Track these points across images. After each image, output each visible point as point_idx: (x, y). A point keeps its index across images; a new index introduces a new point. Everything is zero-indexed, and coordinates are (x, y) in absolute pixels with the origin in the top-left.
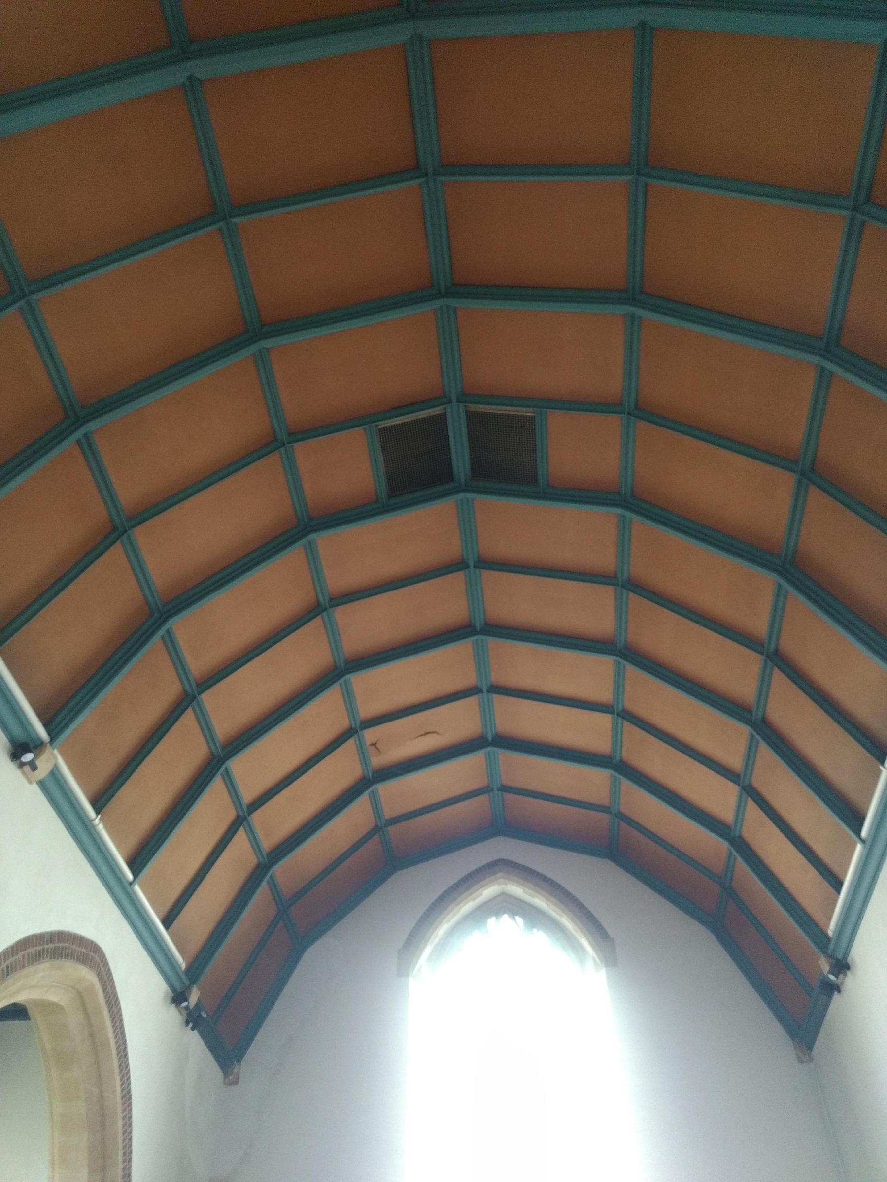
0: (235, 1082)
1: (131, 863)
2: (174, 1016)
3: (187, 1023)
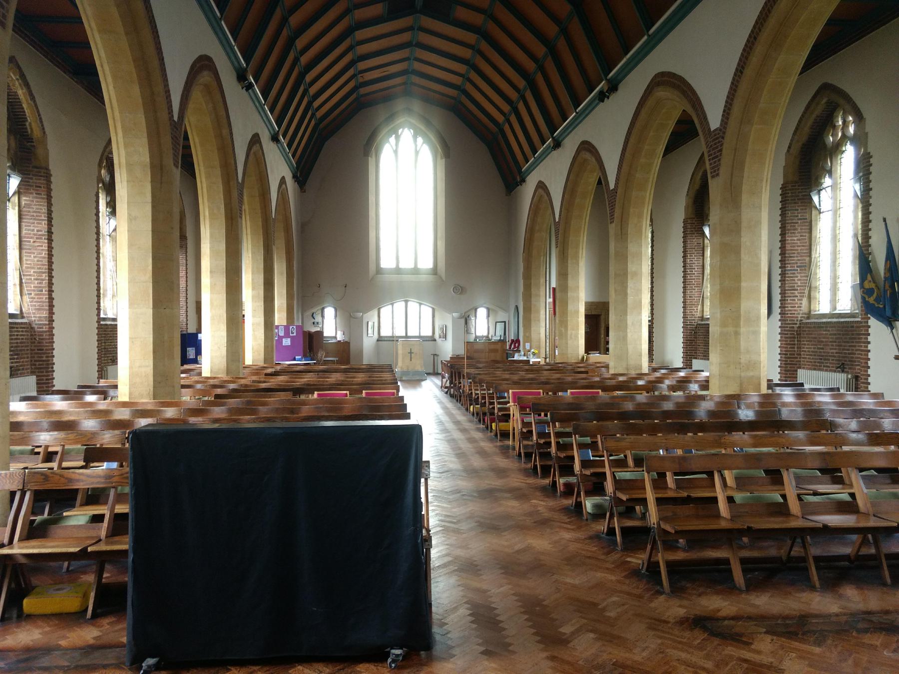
0: (305, 192)
3: (295, 181)
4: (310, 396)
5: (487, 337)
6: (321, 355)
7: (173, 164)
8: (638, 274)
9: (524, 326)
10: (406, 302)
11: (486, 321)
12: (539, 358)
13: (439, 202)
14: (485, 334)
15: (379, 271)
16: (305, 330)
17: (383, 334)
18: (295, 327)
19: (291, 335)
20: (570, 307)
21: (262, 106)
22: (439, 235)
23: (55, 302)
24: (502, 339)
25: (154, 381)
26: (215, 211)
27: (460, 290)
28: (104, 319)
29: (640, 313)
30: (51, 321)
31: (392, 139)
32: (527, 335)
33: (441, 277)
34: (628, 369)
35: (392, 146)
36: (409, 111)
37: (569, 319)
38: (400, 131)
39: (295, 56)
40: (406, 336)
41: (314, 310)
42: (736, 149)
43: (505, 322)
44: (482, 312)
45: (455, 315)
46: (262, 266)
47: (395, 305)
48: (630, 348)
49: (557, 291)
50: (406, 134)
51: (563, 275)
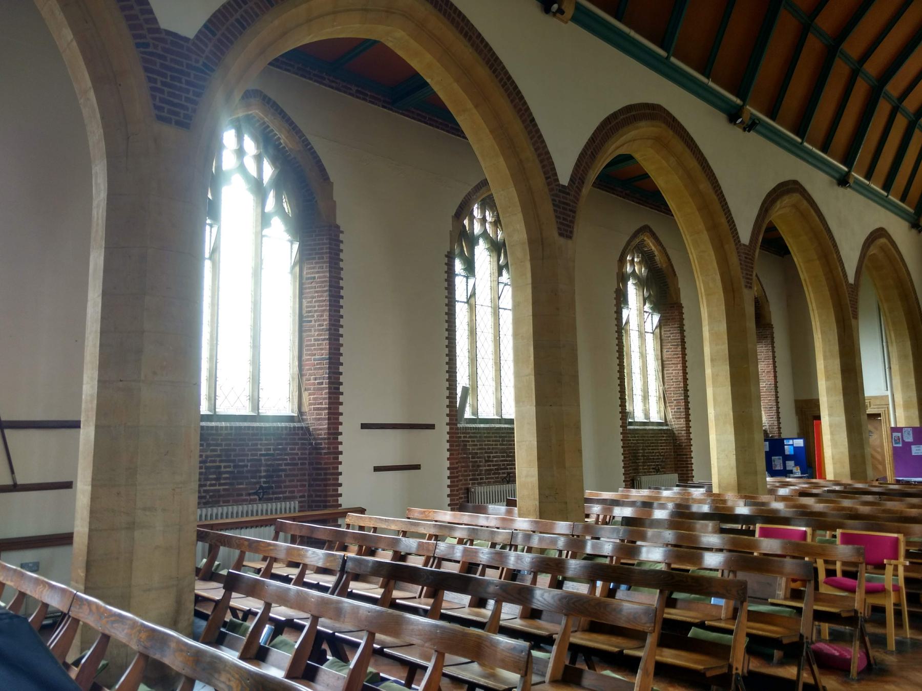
2: (914, 231)
7: (555, 234)
21: (800, 147)
23: (690, 412)
25: (540, 494)
28: (631, 424)
46: (836, 348)
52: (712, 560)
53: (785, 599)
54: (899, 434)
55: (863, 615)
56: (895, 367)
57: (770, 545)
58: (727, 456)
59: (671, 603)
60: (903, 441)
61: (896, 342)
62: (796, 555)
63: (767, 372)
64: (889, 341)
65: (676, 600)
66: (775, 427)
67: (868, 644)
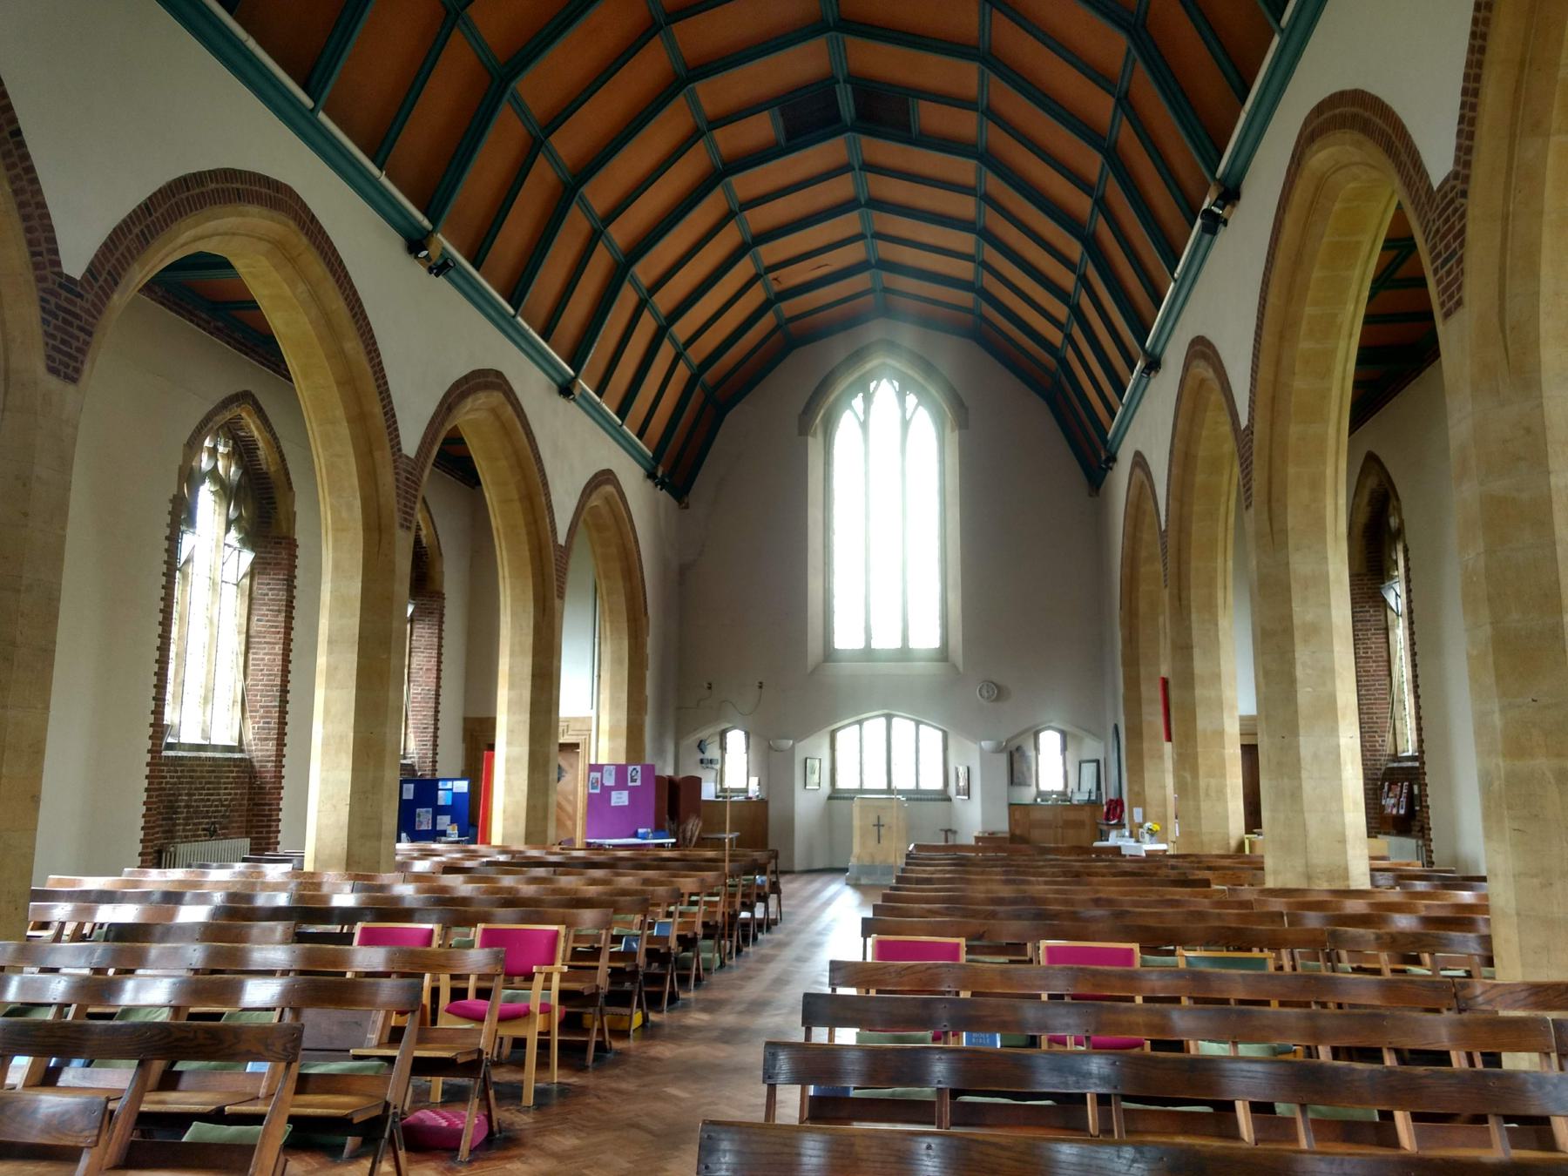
0: (687, 507)
1: (618, 413)
2: (650, 483)
3: (656, 485)
4: (473, 929)
5: (1064, 793)
6: (693, 827)
7: (40, 366)
8: (1319, 631)
9: (1128, 770)
10: (889, 718)
11: (1061, 758)
12: (1165, 841)
13: (949, 515)
14: (1059, 787)
15: (829, 654)
16: (657, 773)
17: (842, 784)
18: (639, 768)
19: (630, 784)
20: (1202, 723)
21: (511, 320)
22: (950, 581)
24: (1093, 798)
26: (345, 514)
27: (999, 693)
28: (170, 747)
29: (1334, 730)
30: (280, 755)
31: (858, 402)
32: (1136, 788)
33: (954, 666)
34: (1309, 878)
35: (856, 415)
36: (891, 346)
37: (1199, 749)
38: (873, 385)
39: (592, 226)
40: (889, 790)
41: (702, 734)
42: (1505, 218)
43: (1098, 762)
44: (1050, 741)
45: (986, 745)
46: (529, 641)
47: (866, 724)
48: (1313, 821)
49: (1171, 683)
50: (885, 391)
51: (1183, 649)
52: (260, 993)
53: (380, 1045)
54: (598, 775)
55: (489, 1056)
56: (605, 676)
57: (367, 958)
58: (335, 806)
59: (170, 1081)
60: (602, 784)
61: (611, 639)
62: (407, 970)
63: (427, 670)
64: (602, 636)
65: (180, 1073)
66: (428, 760)
67: (492, 1101)
